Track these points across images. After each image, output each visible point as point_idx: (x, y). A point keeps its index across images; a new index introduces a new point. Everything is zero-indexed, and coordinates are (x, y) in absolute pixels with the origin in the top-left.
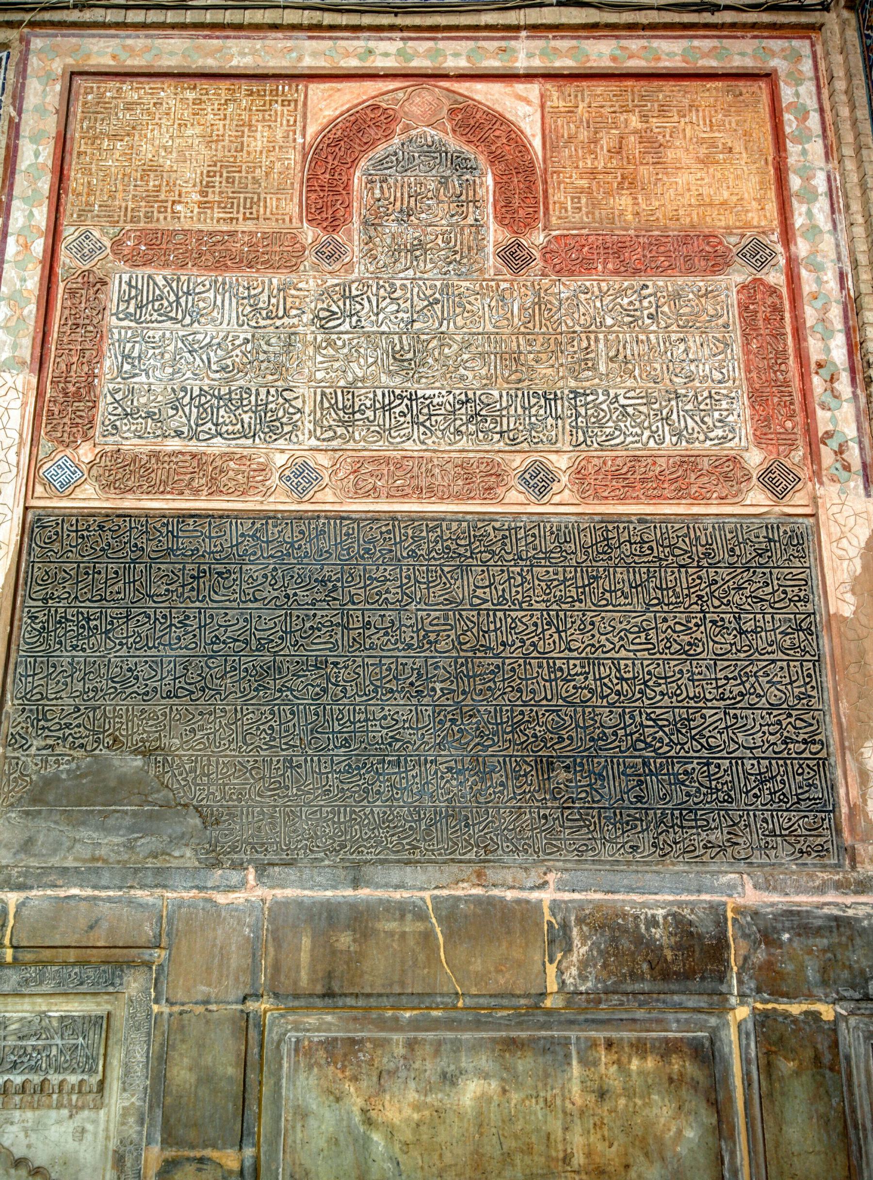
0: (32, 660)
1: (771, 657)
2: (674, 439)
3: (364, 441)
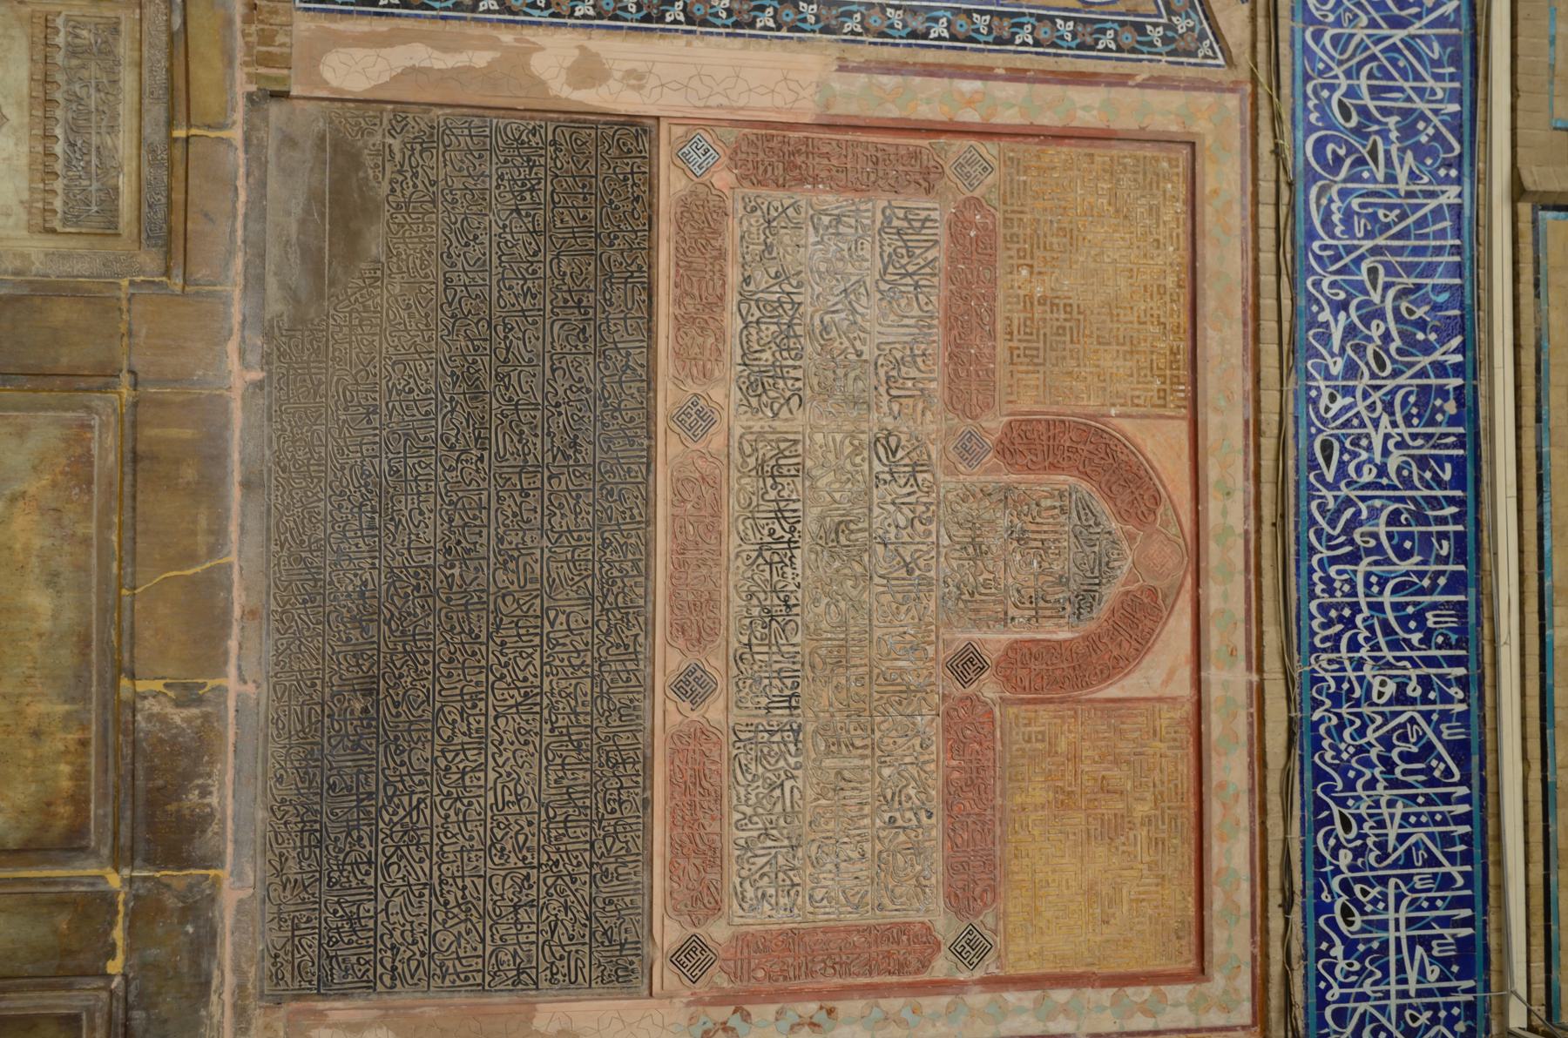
1: (488, 939)
2: (742, 842)
3: (739, 488)
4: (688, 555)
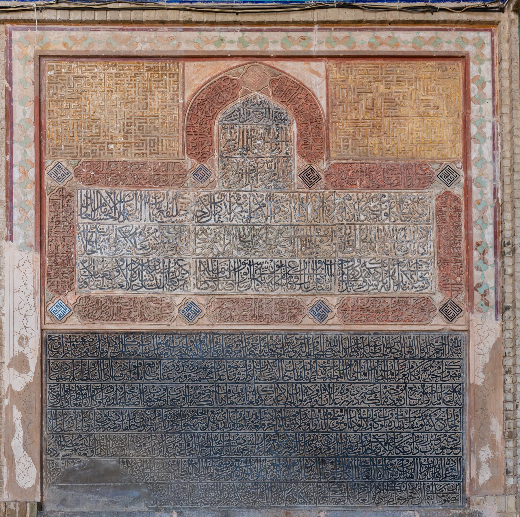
2: (396, 288)
3: (225, 290)
4: (257, 314)
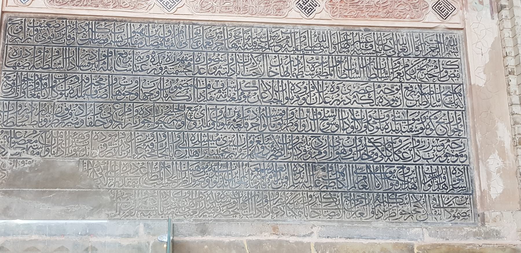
0: (7, 102)
1: (439, 108)
